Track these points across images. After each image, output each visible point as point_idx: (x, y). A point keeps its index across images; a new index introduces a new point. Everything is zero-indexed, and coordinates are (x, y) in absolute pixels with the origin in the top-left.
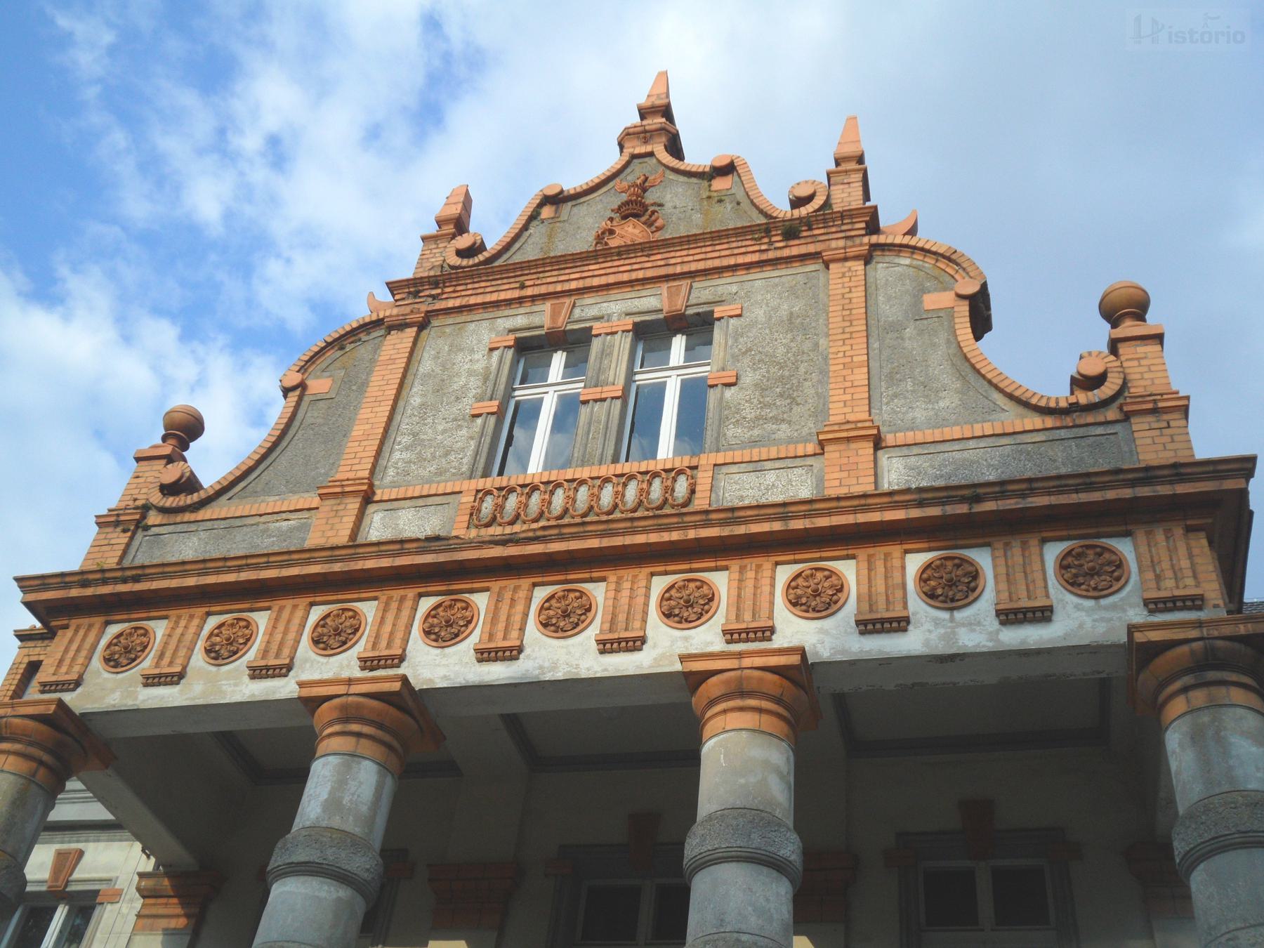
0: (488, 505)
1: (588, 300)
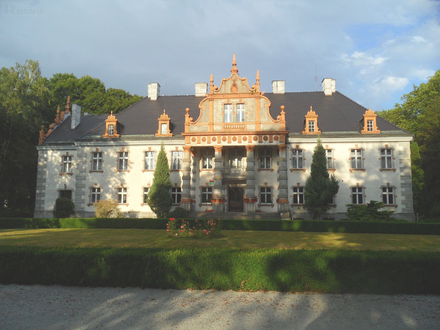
0: (225, 126)
1: (231, 99)
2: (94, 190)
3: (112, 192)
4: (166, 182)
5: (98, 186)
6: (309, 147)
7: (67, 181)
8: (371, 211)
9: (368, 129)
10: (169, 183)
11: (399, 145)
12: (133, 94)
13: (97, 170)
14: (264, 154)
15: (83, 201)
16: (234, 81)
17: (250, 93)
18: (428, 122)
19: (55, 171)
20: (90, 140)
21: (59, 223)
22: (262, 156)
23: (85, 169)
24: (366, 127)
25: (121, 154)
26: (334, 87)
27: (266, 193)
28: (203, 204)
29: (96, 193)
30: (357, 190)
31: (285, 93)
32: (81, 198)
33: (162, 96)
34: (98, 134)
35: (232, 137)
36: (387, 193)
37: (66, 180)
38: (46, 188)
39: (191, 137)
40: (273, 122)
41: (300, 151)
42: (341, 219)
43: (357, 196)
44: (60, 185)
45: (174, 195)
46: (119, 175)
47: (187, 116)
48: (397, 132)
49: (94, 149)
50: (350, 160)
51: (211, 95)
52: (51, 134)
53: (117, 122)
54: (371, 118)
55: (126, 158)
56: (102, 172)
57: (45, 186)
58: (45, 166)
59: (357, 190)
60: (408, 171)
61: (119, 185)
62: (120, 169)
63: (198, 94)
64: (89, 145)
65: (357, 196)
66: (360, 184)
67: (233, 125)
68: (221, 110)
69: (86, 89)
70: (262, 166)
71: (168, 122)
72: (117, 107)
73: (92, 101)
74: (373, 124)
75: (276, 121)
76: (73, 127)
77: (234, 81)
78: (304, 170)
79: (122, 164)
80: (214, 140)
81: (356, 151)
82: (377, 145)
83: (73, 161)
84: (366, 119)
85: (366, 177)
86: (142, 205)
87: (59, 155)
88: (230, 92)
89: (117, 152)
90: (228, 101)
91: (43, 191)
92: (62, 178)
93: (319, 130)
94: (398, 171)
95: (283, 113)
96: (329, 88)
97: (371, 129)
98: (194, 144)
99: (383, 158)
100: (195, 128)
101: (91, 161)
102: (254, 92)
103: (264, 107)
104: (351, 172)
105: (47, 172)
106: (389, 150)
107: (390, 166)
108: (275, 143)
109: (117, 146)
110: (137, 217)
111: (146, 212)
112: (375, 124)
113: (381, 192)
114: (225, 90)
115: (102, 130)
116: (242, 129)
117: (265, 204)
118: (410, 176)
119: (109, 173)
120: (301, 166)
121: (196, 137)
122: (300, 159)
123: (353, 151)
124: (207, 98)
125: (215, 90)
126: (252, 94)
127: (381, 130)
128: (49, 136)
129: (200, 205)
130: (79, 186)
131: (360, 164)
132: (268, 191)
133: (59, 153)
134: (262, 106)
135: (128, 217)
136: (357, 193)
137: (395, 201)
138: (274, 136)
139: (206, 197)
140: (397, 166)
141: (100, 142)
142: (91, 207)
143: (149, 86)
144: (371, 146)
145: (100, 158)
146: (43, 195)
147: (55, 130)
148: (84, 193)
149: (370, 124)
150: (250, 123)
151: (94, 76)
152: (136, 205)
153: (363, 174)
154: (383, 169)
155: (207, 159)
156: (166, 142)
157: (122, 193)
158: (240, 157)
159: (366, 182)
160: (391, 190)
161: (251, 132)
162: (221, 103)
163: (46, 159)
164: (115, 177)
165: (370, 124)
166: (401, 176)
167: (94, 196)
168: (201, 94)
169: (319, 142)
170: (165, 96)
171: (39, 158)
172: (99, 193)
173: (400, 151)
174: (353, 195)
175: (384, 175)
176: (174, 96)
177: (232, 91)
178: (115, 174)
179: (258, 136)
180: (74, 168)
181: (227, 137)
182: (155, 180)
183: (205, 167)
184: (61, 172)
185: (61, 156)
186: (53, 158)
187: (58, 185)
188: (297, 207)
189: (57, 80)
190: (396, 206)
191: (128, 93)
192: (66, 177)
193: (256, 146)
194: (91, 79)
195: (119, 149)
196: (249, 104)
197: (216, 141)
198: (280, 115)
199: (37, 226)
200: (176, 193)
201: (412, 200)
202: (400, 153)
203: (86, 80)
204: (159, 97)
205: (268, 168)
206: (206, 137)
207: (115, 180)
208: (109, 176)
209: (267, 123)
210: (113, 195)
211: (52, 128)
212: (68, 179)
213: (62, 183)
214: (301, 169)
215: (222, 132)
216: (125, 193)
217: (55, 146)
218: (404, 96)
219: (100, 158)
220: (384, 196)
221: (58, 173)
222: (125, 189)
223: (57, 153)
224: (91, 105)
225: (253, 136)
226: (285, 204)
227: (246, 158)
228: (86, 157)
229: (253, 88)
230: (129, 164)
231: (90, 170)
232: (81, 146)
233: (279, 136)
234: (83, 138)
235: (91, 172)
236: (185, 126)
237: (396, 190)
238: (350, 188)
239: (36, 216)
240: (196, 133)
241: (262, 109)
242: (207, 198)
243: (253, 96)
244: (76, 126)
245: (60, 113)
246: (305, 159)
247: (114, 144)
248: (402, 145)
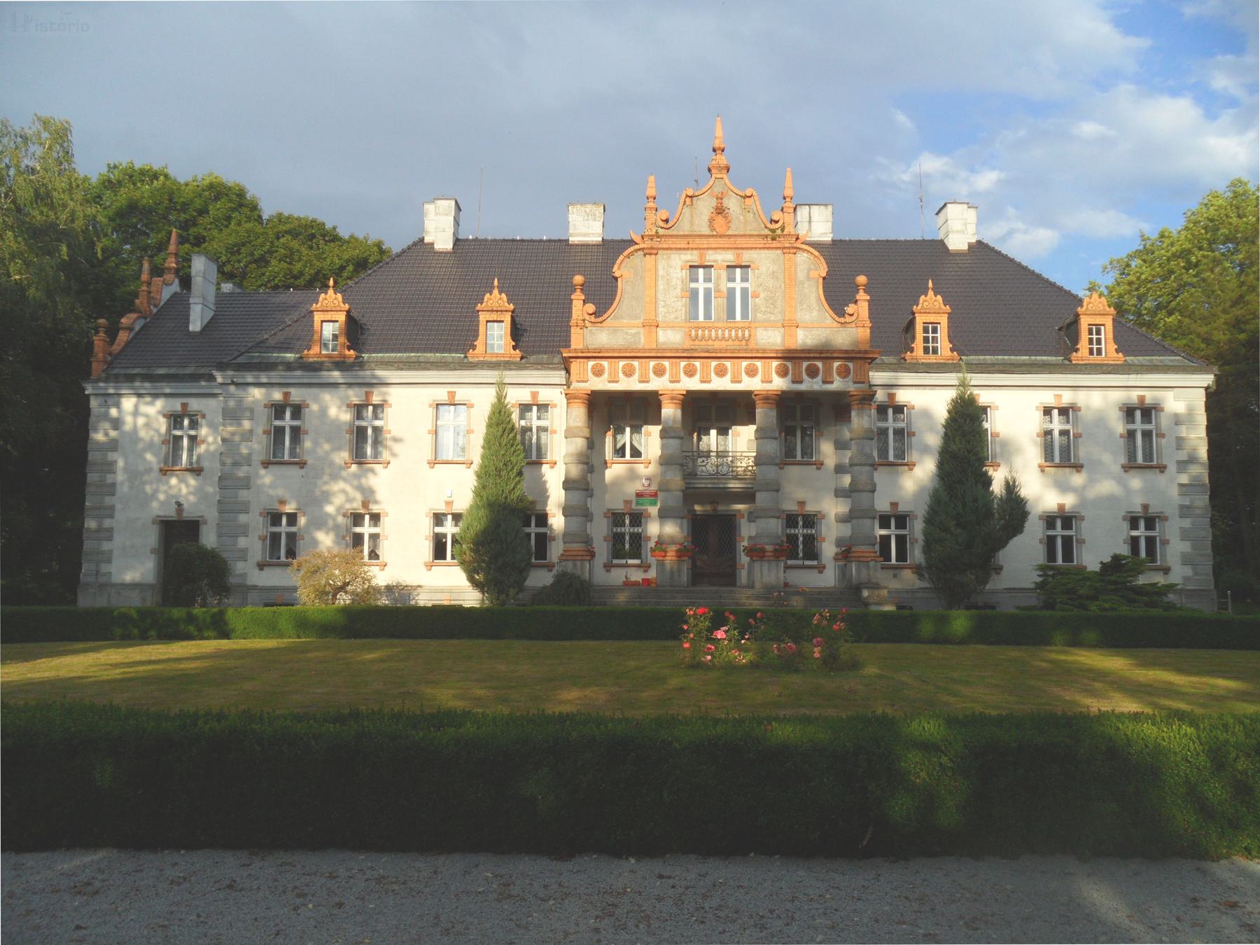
0: (693, 333)
1: (710, 252)
2: (275, 518)
3: (336, 528)
4: (514, 496)
5: (289, 508)
6: (928, 400)
7: (184, 490)
8: (1115, 583)
9: (1091, 352)
10: (521, 501)
11: (1176, 398)
12: (344, 233)
13: (286, 457)
14: (800, 417)
15: (243, 555)
16: (720, 199)
17: (767, 236)
18: (1199, 335)
19: (145, 459)
20: (270, 366)
21: (226, 623)
22: (789, 423)
23: (250, 455)
24: (1083, 344)
25: (359, 410)
26: (972, 229)
27: (800, 531)
28: (616, 561)
29: (284, 527)
30: (1059, 523)
31: (835, 243)
33: (467, 240)
34: (287, 350)
35: (714, 363)
36: (1141, 532)
37: (182, 488)
38: (117, 515)
39: (591, 363)
40: (835, 324)
41: (899, 409)
42: (1018, 608)
43: (1059, 542)
44: (162, 503)
45: (529, 535)
46: (357, 476)
47: (577, 298)
48: (1167, 359)
49: (277, 395)
50: (1039, 439)
51: (651, 238)
52: (128, 344)
53: (348, 312)
54: (1098, 320)
55: (377, 423)
56: (302, 464)
57: (112, 508)
58: (113, 445)
59: (1059, 523)
60: (1200, 471)
61: (357, 506)
62: (359, 457)
63: (579, 235)
64: (264, 380)
65: (1059, 542)
66: (1067, 508)
67: (717, 329)
68: (679, 283)
69: (207, 212)
70: (790, 453)
71: (507, 318)
72: (309, 272)
73: (234, 250)
74: (1103, 337)
75: (842, 320)
76: (195, 326)
77: (720, 199)
78: (911, 466)
79: (364, 441)
80: (659, 372)
81: (1055, 412)
82: (1118, 396)
83: (204, 431)
84: (1084, 322)
85: (1084, 487)
86: (429, 566)
87: (159, 412)
88: (706, 231)
89: (348, 406)
90: (701, 256)
91: (107, 523)
92: (167, 482)
93: (952, 350)
94: (1172, 468)
95: (862, 296)
96: (959, 230)
97: (1099, 352)
98: (601, 384)
99: (1131, 434)
100: (600, 337)
101: (266, 432)
102: (779, 232)
103: (808, 278)
104: (1043, 471)
105: (121, 463)
106: (1148, 411)
107: (1148, 455)
108: (837, 384)
109: (350, 385)
110: (413, 603)
111: (450, 585)
112: (1110, 335)
113: (1125, 531)
114: (692, 223)
115: (307, 335)
116: (744, 343)
117: (800, 562)
118: (1204, 485)
119: (327, 470)
120: (900, 454)
121: (605, 363)
122: (899, 433)
123: (1047, 411)
124: (636, 247)
125: (662, 224)
126: (773, 239)
127: (1126, 353)
128: (123, 350)
129: (608, 567)
130: (229, 507)
131: (1066, 451)
132: (805, 526)
133: (159, 404)
134: (801, 275)
135: (384, 601)
136: (1059, 531)
137: (1164, 555)
138: (836, 364)
139: (626, 542)
140: (1170, 457)
141: (299, 373)
142: (268, 572)
143: (426, 206)
144: (1101, 398)
145: (296, 423)
146: (108, 534)
147: (138, 333)
148: (244, 531)
149: (1095, 337)
150: (768, 325)
151: (230, 176)
152: (415, 565)
153: (1078, 479)
154: (1131, 466)
155: (628, 430)
156: (510, 376)
157: (366, 529)
158: (724, 425)
159: (1083, 502)
160: (1150, 523)
161: (772, 351)
162: (680, 263)
163: (117, 423)
164: (345, 480)
165: (1095, 337)
166: (1181, 485)
167: (275, 538)
168: (585, 235)
169: (963, 384)
170: (476, 240)
171: (92, 419)
172: (293, 529)
173: (1176, 415)
174: (1049, 537)
175: (1136, 482)
176: (504, 240)
177: (713, 229)
178: (344, 473)
179: (789, 364)
180: (207, 451)
181: (697, 363)
182: (478, 493)
183: (620, 452)
184: (166, 462)
185: (164, 416)
186: (141, 421)
187: (155, 504)
188: (891, 572)
189: (119, 182)
190: (1166, 570)
191: (334, 228)
192: (181, 481)
193: (783, 392)
194: (222, 185)
195: (355, 396)
196: (763, 269)
197: (667, 376)
198: (856, 302)
199: (153, 633)
200: (533, 529)
201: (1209, 551)
202: (1177, 420)
203: (211, 186)
204: (457, 241)
205: (809, 458)
206: (636, 363)
207: (344, 491)
208: (326, 478)
209: (814, 324)
210: (337, 535)
211: (130, 329)
212: (187, 485)
213: (169, 497)
214: (901, 462)
215: (684, 350)
216: (374, 530)
217: (147, 385)
218: (1111, 263)
219: (296, 423)
220: (1134, 541)
221: (156, 467)
222: (376, 518)
223: (151, 403)
224: (229, 261)
225: (775, 363)
226: (872, 564)
227: (753, 428)
228: (251, 419)
229: (777, 222)
231: (263, 457)
232: (237, 384)
233: (851, 365)
234: (239, 360)
235: (266, 464)
236: (573, 330)
237: (1167, 524)
238: (1041, 518)
239: (85, 601)
240: (607, 350)
241: (802, 283)
242: (627, 546)
243: (775, 244)
244: (205, 322)
245: (149, 284)
246: (912, 434)
247: (341, 381)
248: (1184, 397)
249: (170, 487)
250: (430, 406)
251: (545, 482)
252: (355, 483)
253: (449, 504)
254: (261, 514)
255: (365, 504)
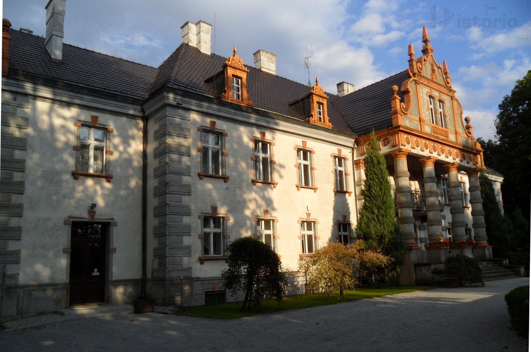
15: (188, 250)
32: (181, 243)
40: (467, 137)
56: (225, 179)
61: (260, 213)
83: (116, 141)
92: (83, 183)
133: (73, 112)
148: (187, 230)
192: (96, 183)
207: (255, 200)
212: (102, 187)
230: (276, 167)
247: (252, 121)
249: (86, 188)
250: (295, 148)
251: (348, 204)
252: (261, 194)
253: (308, 215)
254: (199, 217)
255: (266, 212)
